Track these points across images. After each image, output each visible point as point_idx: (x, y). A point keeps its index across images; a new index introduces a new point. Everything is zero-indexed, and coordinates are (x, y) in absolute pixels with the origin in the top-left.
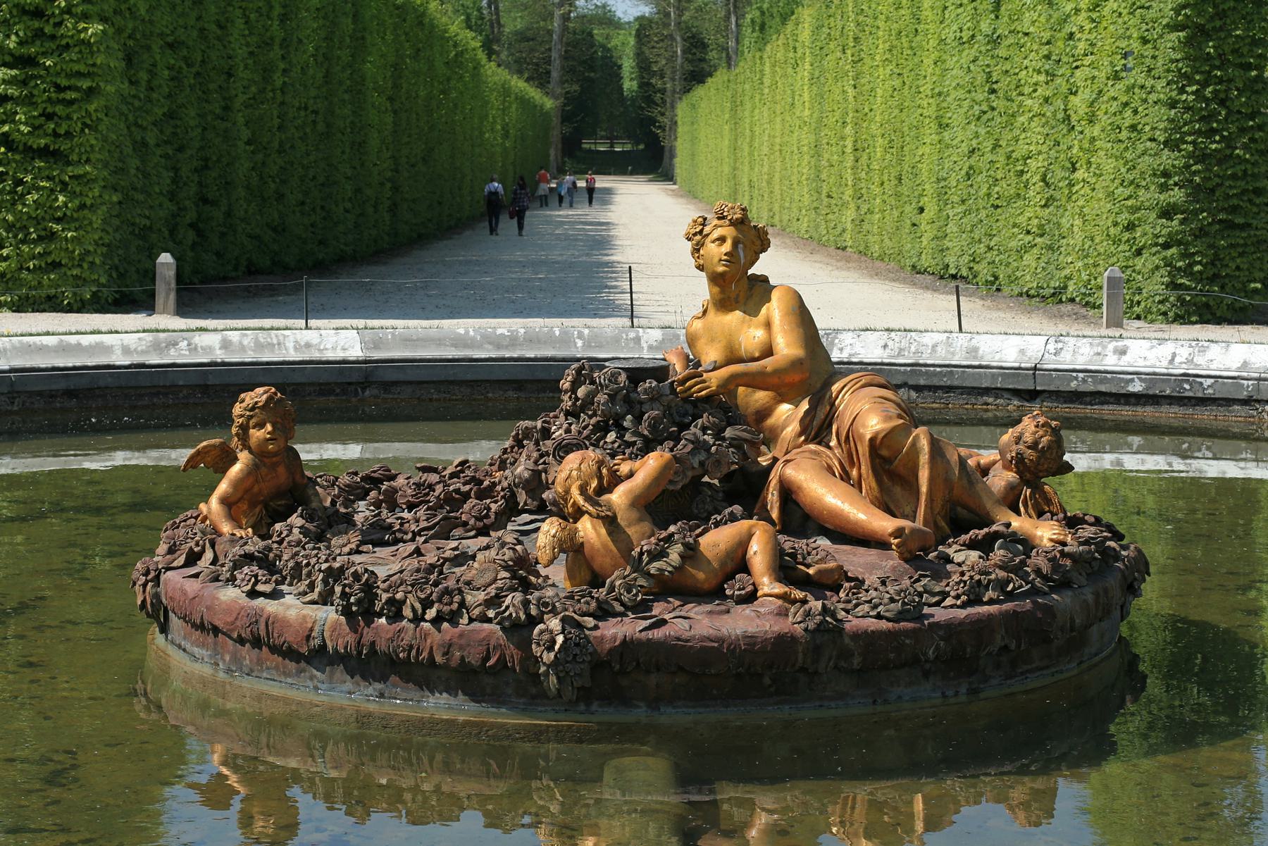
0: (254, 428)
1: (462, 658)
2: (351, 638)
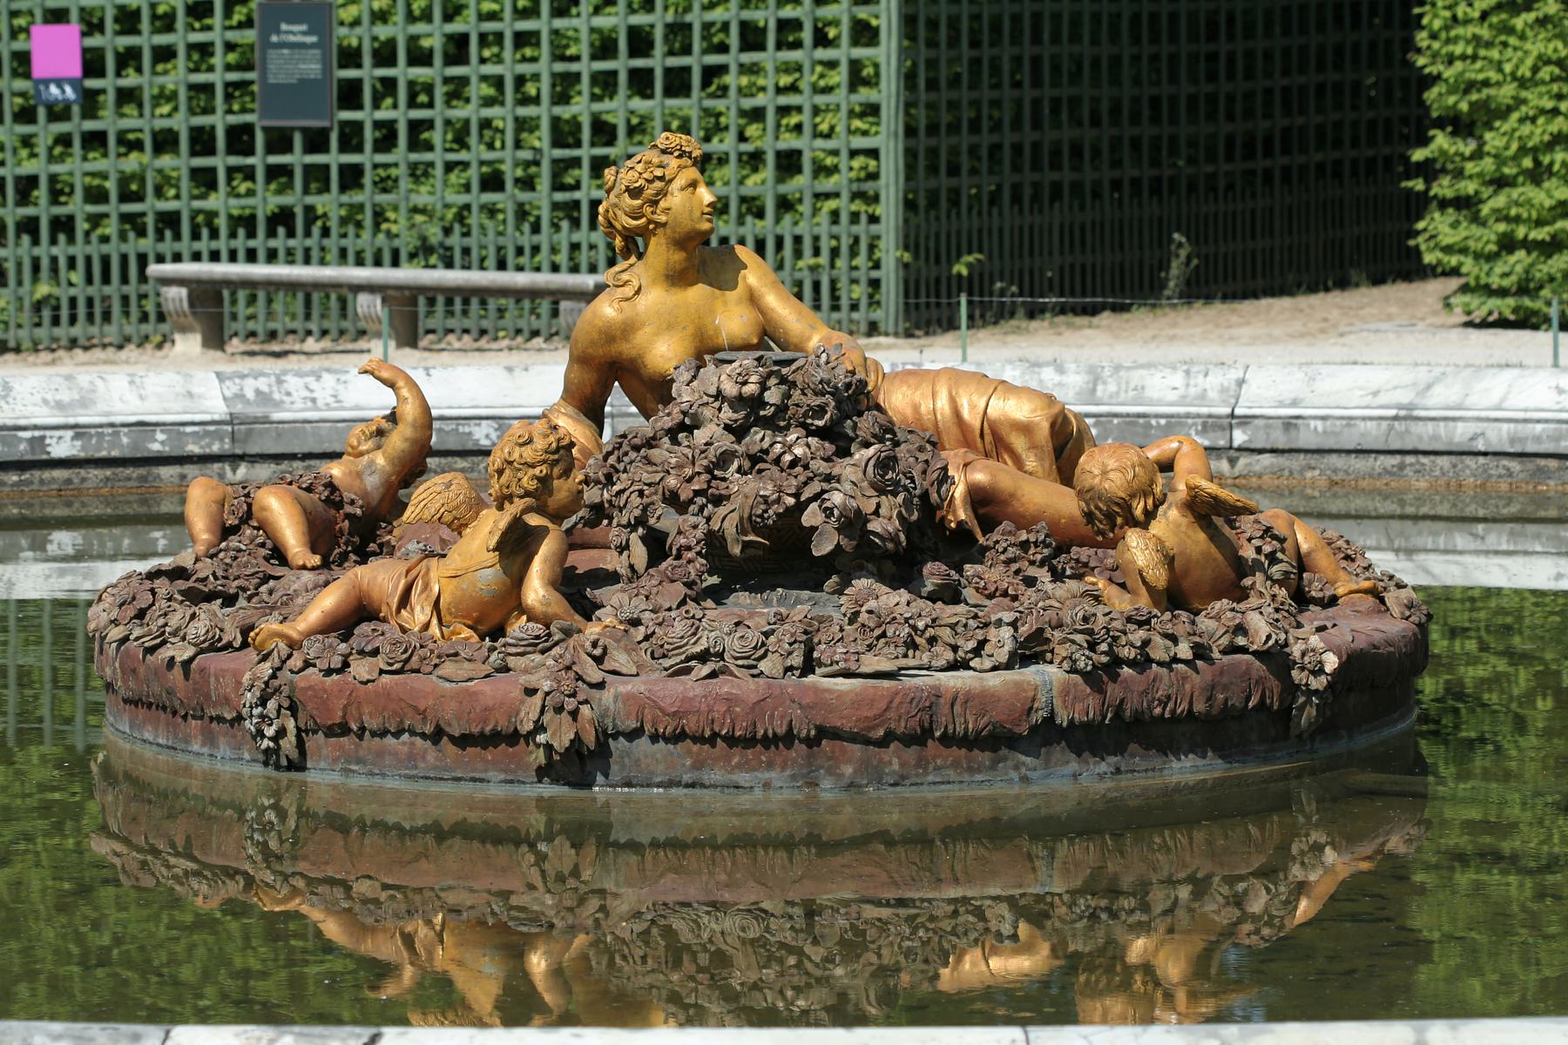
0: (559, 478)
1: (1226, 700)
2: (1093, 702)
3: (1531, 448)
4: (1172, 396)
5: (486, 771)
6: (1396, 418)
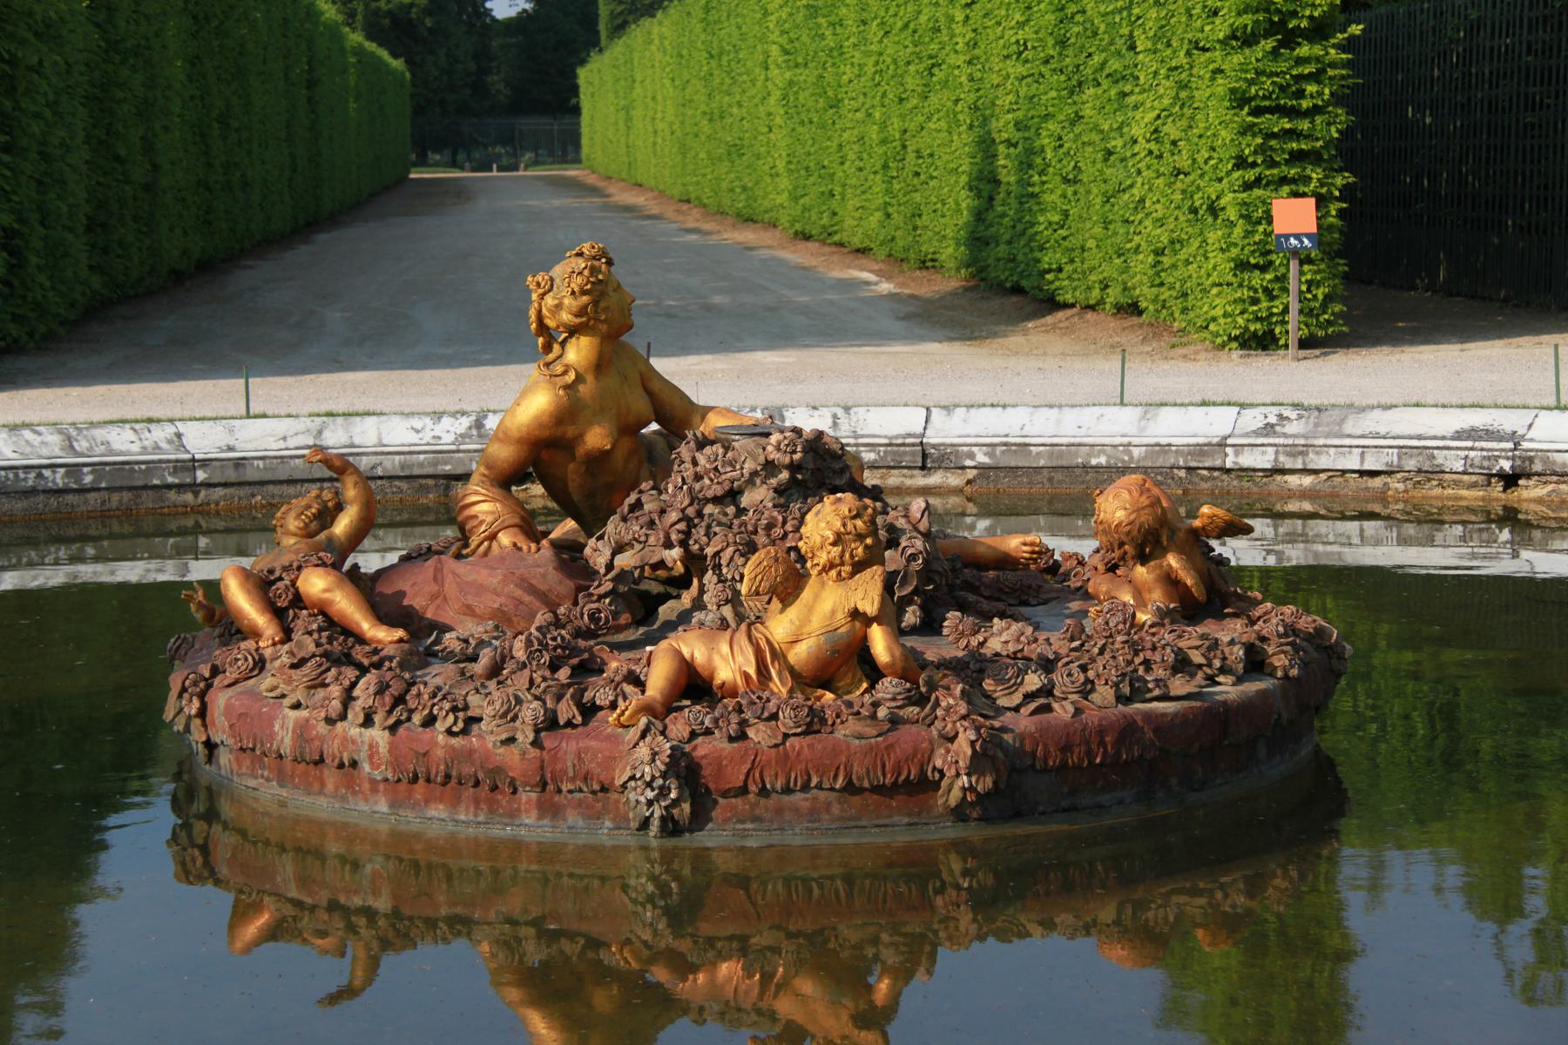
3: (416, 472)
5: (890, 816)
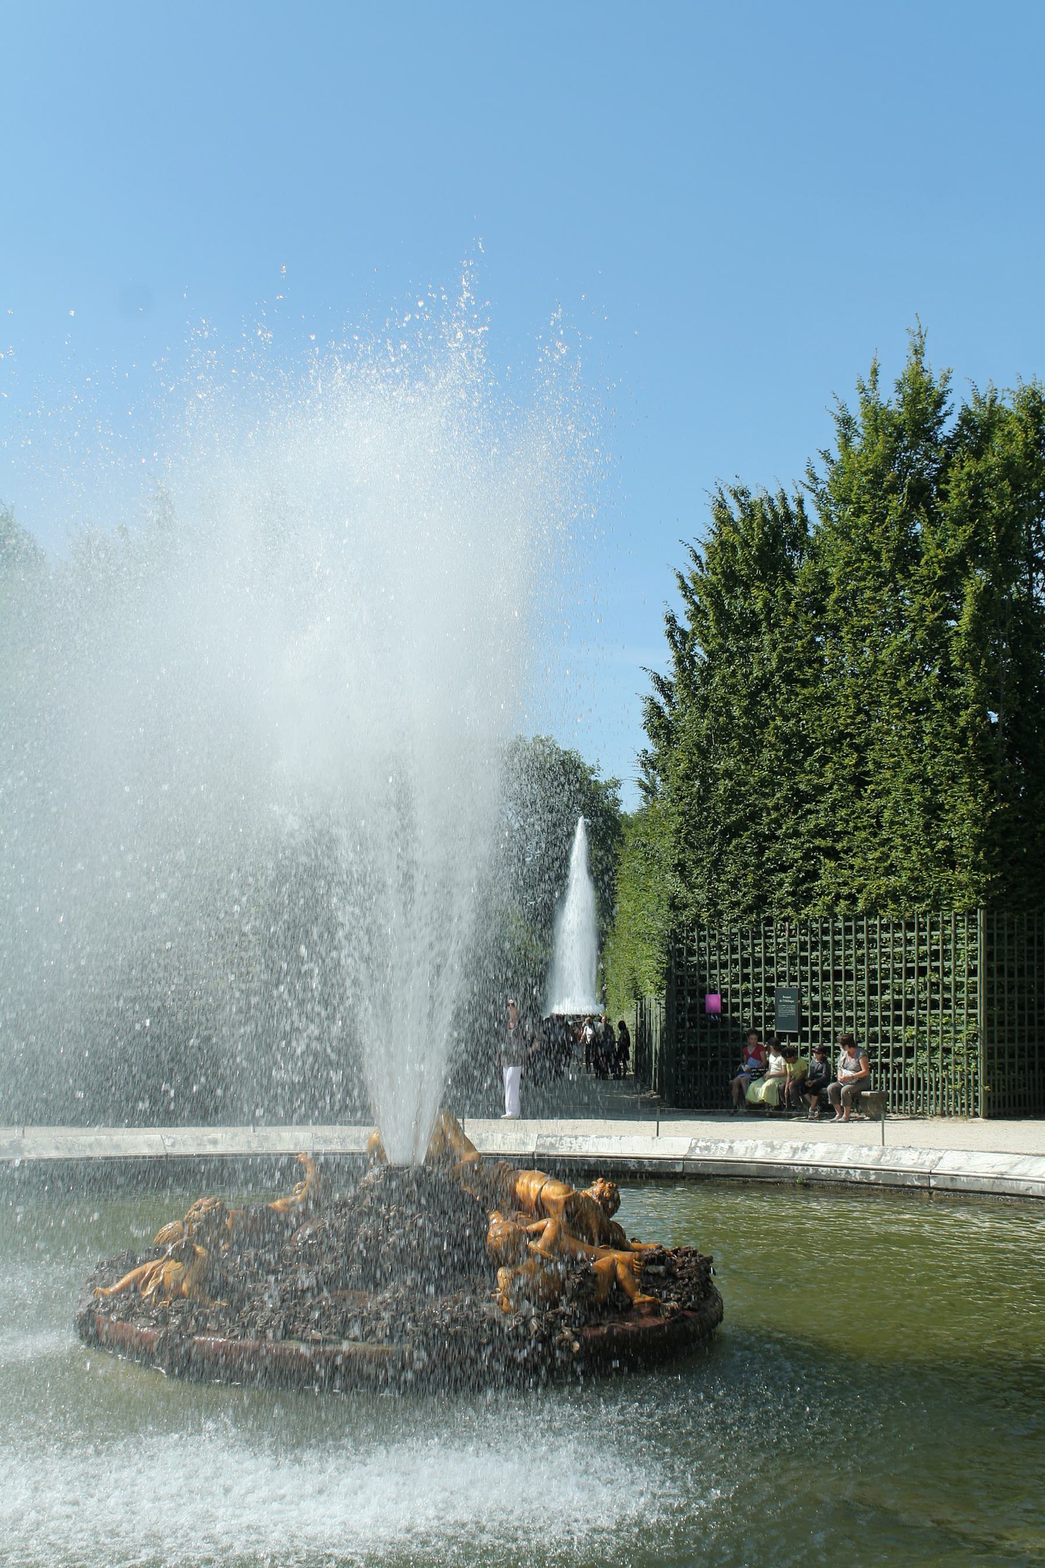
4: (911, 1163)
6: (996, 1178)
